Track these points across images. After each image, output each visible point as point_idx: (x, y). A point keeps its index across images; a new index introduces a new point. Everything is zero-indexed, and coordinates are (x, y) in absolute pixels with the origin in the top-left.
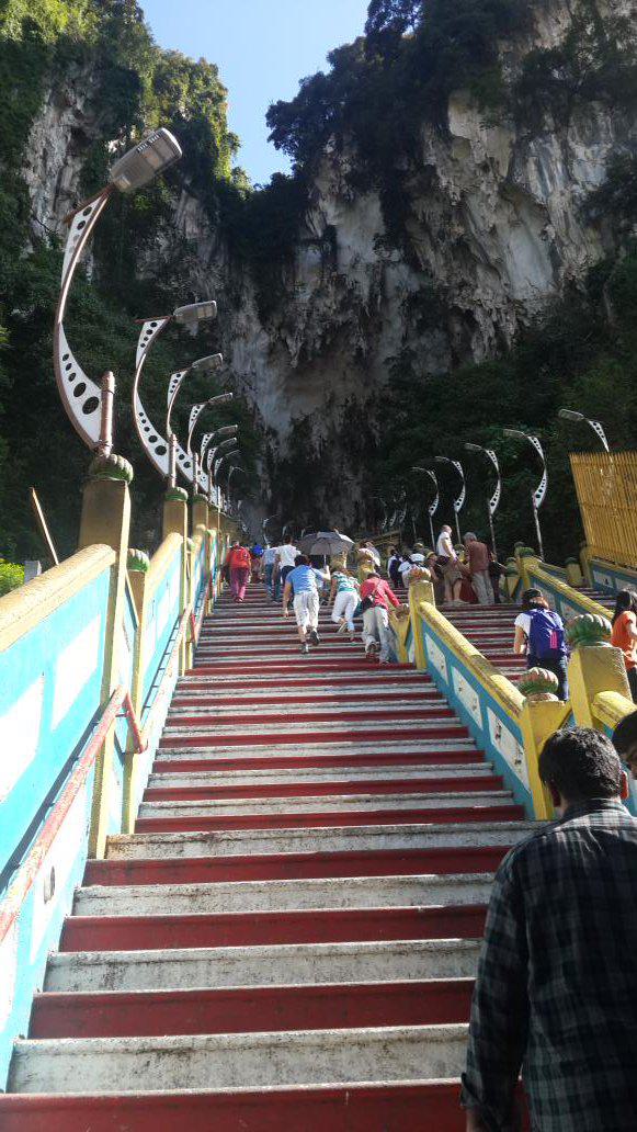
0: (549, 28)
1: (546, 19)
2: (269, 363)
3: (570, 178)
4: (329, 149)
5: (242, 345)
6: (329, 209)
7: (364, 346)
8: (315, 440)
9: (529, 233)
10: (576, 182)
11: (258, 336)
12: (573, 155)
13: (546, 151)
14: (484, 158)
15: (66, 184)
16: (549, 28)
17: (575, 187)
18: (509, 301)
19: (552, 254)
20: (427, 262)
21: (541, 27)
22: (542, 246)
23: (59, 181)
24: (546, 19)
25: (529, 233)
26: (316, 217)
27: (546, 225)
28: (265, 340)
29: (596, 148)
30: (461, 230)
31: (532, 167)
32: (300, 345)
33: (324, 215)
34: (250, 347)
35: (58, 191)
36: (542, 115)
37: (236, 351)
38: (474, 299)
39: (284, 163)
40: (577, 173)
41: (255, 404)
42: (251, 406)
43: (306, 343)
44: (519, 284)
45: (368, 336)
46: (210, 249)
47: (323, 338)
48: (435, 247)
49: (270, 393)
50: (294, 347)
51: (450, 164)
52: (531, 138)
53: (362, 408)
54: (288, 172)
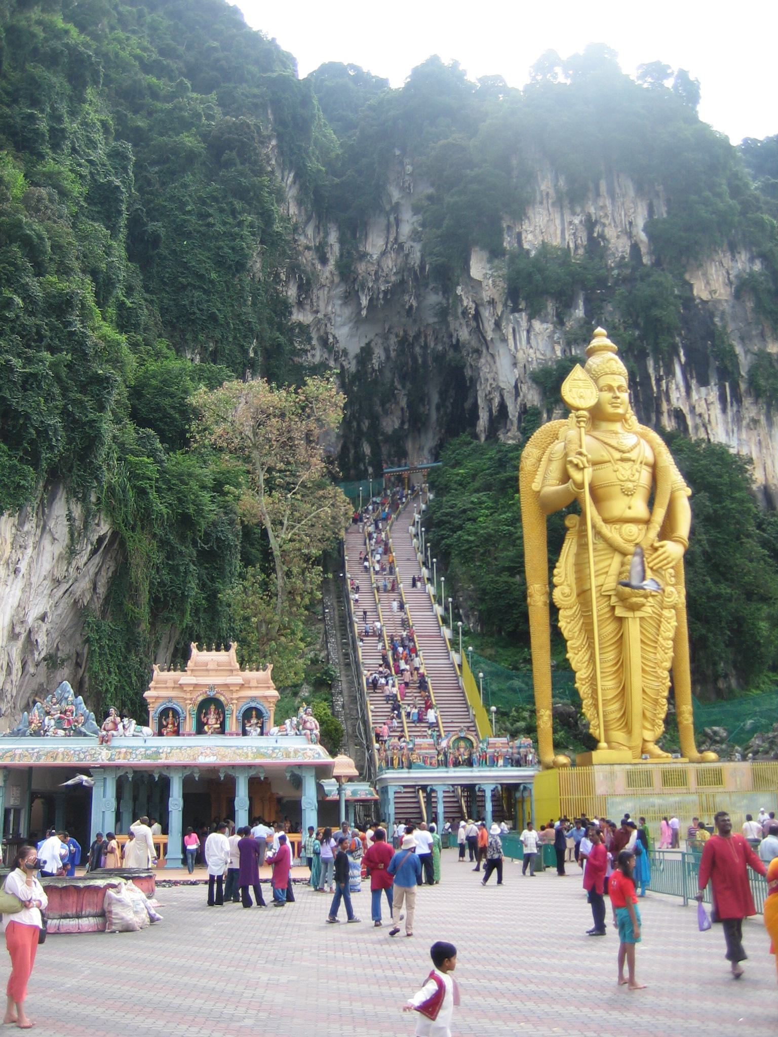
5: (326, 292)
7: (415, 304)
10: (531, 347)
11: (338, 285)
12: (534, 330)
13: (518, 322)
17: (531, 351)
21: (530, 213)
28: (340, 290)
29: (545, 326)
31: (511, 330)
33: (390, 196)
37: (321, 296)
40: (533, 342)
41: (334, 337)
42: (331, 340)
44: (501, 378)
47: (386, 293)
49: (344, 325)
50: (364, 302)
53: (411, 339)
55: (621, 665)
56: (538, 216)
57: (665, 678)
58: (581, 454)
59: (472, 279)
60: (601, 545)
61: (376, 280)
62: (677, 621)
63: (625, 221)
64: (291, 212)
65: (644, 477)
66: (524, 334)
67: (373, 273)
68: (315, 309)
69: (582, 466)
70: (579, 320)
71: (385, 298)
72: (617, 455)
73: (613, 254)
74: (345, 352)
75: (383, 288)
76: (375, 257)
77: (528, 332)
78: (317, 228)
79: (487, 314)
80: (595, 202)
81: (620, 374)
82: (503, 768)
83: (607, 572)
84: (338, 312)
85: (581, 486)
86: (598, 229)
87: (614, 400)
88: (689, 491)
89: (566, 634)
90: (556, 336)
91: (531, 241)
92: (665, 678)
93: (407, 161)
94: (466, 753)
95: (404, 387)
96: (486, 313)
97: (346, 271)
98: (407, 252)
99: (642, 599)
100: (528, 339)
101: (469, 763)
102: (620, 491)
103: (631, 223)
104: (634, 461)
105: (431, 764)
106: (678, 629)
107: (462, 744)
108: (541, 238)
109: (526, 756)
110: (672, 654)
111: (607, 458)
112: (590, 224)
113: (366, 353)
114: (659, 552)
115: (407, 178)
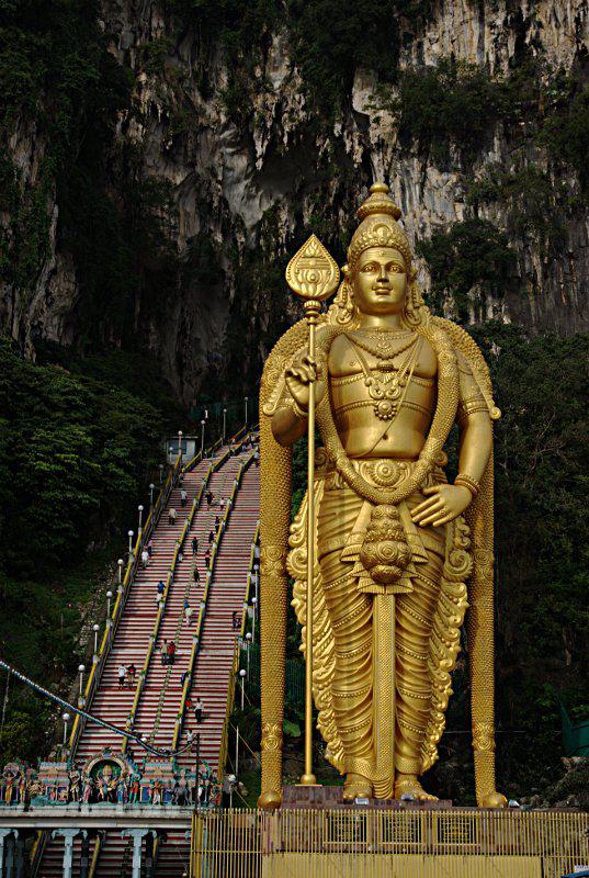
11: (226, 127)
14: (376, 139)
16: (443, 15)
17: (425, 213)
29: (445, 176)
31: (398, 184)
32: (266, 143)
37: (203, 142)
42: (215, 204)
50: (260, 150)
52: (400, 158)
53: (331, 200)
55: (369, 661)
56: (448, 17)
57: (445, 683)
58: (307, 362)
59: (355, 112)
60: (349, 492)
61: (277, 119)
62: (469, 600)
63: (571, 19)
64: (154, 23)
65: (417, 391)
67: (274, 106)
68: (189, 160)
69: (304, 378)
70: (490, 168)
72: (372, 363)
73: (549, 68)
74: (240, 219)
76: (277, 85)
77: (422, 185)
78: (196, 45)
79: (375, 163)
81: (392, 247)
82: (160, 807)
83: (350, 529)
84: (228, 164)
85: (304, 407)
86: (531, 32)
87: (380, 284)
88: (496, 413)
89: (300, 616)
90: (458, 191)
91: (433, 51)
92: (445, 683)
94: (113, 783)
96: (376, 159)
97: (237, 103)
99: (393, 568)
100: (422, 195)
101: (112, 797)
102: (373, 414)
104: (397, 370)
105: (59, 797)
106: (469, 614)
107: (107, 769)
108: (450, 49)
109: (195, 790)
110: (459, 648)
111: (357, 366)
112: (518, 25)
114: (431, 499)
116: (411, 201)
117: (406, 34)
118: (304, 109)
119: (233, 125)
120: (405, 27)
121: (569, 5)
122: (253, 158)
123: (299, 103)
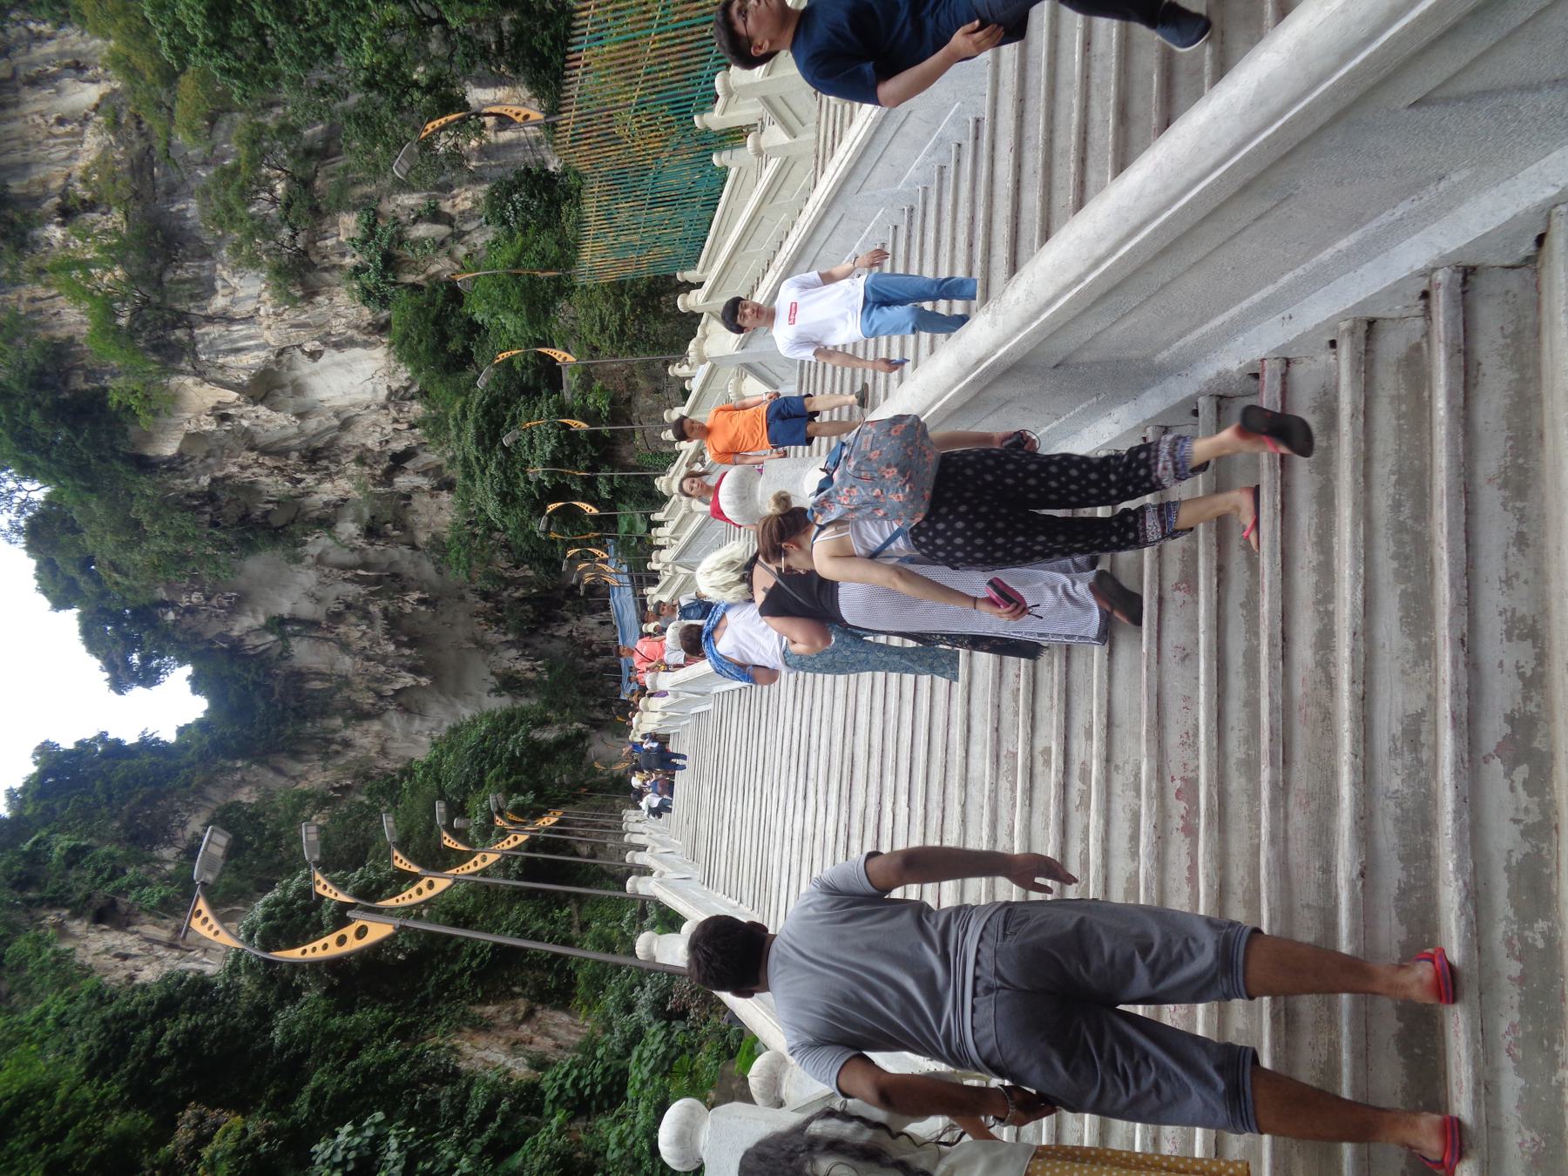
0: (62, 326)
1: (52, 327)
2: (422, 714)
3: (249, 319)
4: (171, 616)
6: (244, 624)
7: (416, 595)
8: (522, 665)
9: (311, 374)
10: (257, 310)
11: (387, 725)
12: (225, 310)
15: (165, 935)
17: (262, 312)
18: (385, 407)
19: (338, 346)
20: (327, 504)
21: (61, 334)
22: (330, 356)
23: (159, 942)
24: (52, 327)
25: (311, 374)
26: (252, 641)
27: (304, 352)
28: (395, 720)
29: (219, 284)
30: (295, 455)
31: (231, 359)
34: (398, 734)
35: (171, 946)
36: (170, 342)
37: (401, 753)
38: (377, 449)
39: (179, 677)
43: (403, 666)
44: (368, 396)
45: (404, 589)
46: (271, 775)
47: (399, 645)
48: (307, 493)
50: (407, 680)
51: (211, 461)
52: (195, 354)
54: (188, 670)
59: (180, 454)
61: (383, 660)
66: (238, 330)
71: (409, 645)
75: (392, 647)
77: (232, 321)
80: (36, 201)
84: (433, 724)
93: (184, 601)
95: (566, 620)
98: (342, 607)
103: (61, 121)
113: (509, 683)
115: (214, 602)
116: (250, 338)
117: (86, 380)
118: (371, 625)
119: (386, 717)
120: (79, 383)
121: (51, 142)
122: (418, 687)
123: (365, 633)
